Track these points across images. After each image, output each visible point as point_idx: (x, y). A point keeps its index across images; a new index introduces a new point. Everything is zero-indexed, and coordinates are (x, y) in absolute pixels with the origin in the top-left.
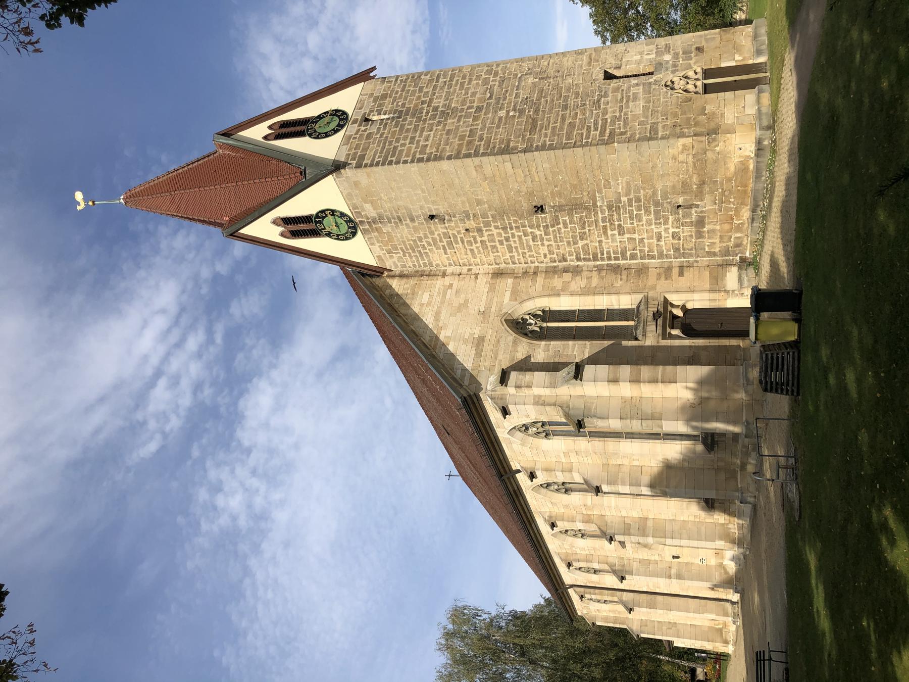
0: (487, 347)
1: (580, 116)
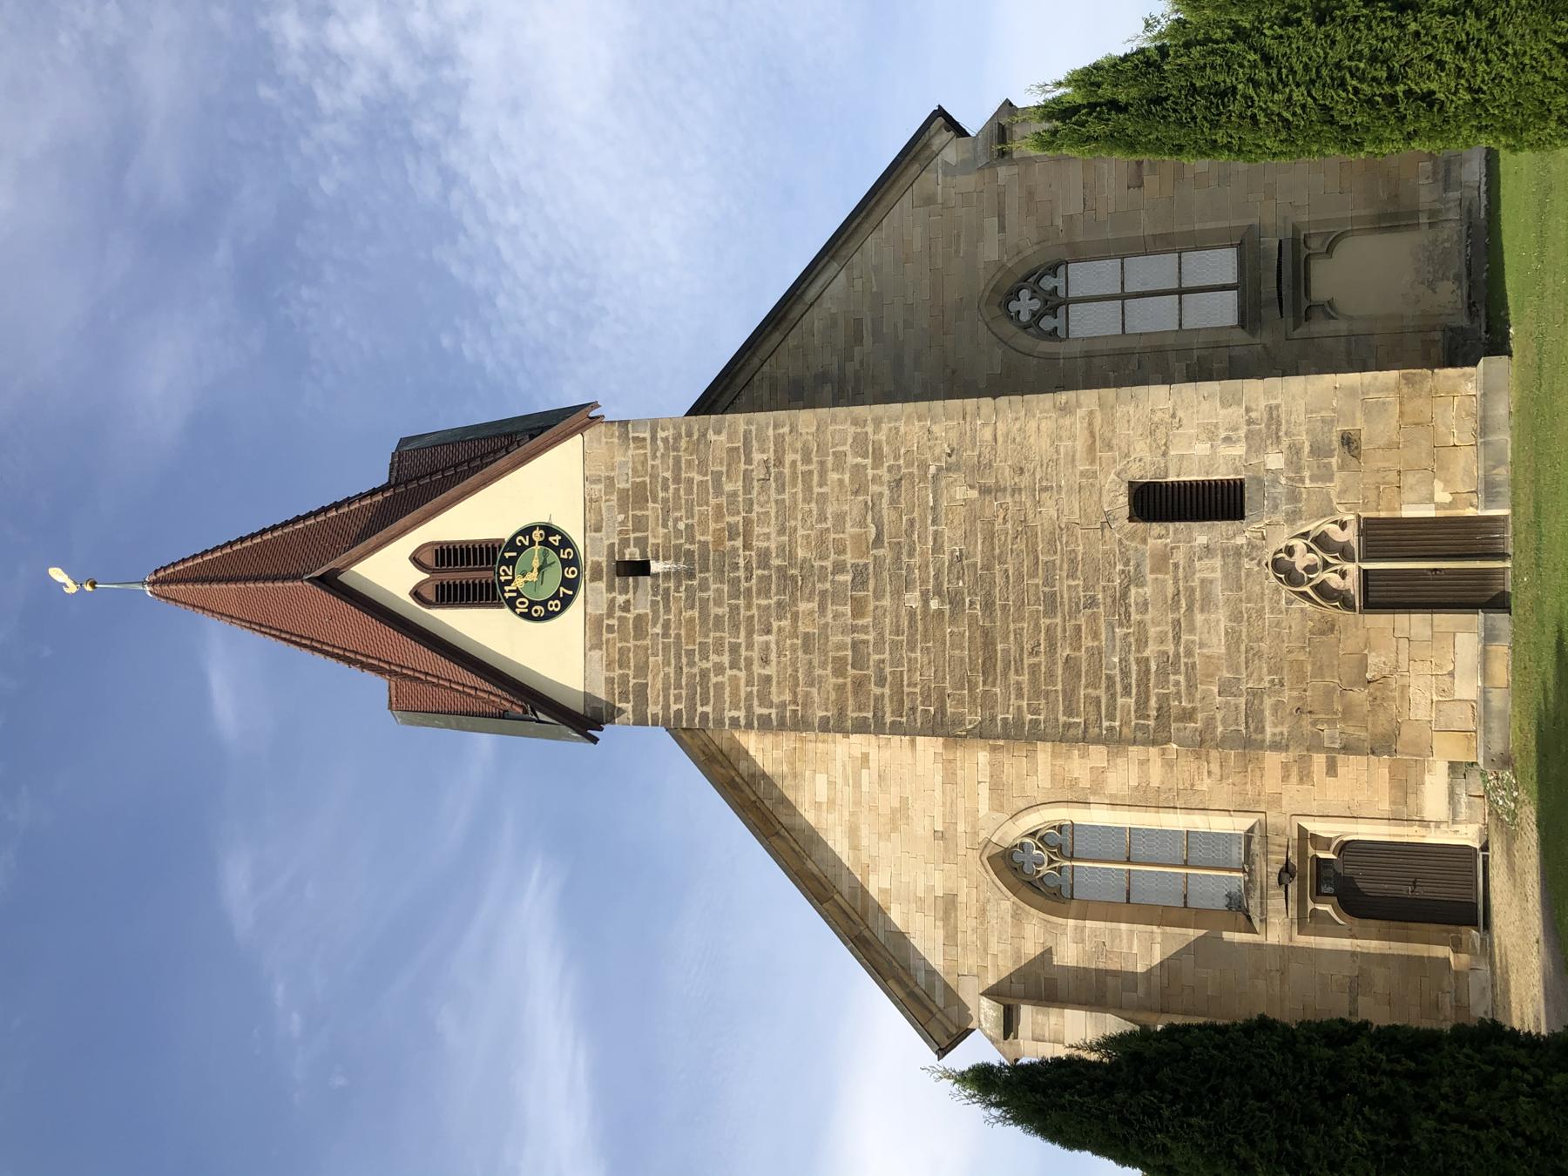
0: (966, 921)
1: (1087, 642)
